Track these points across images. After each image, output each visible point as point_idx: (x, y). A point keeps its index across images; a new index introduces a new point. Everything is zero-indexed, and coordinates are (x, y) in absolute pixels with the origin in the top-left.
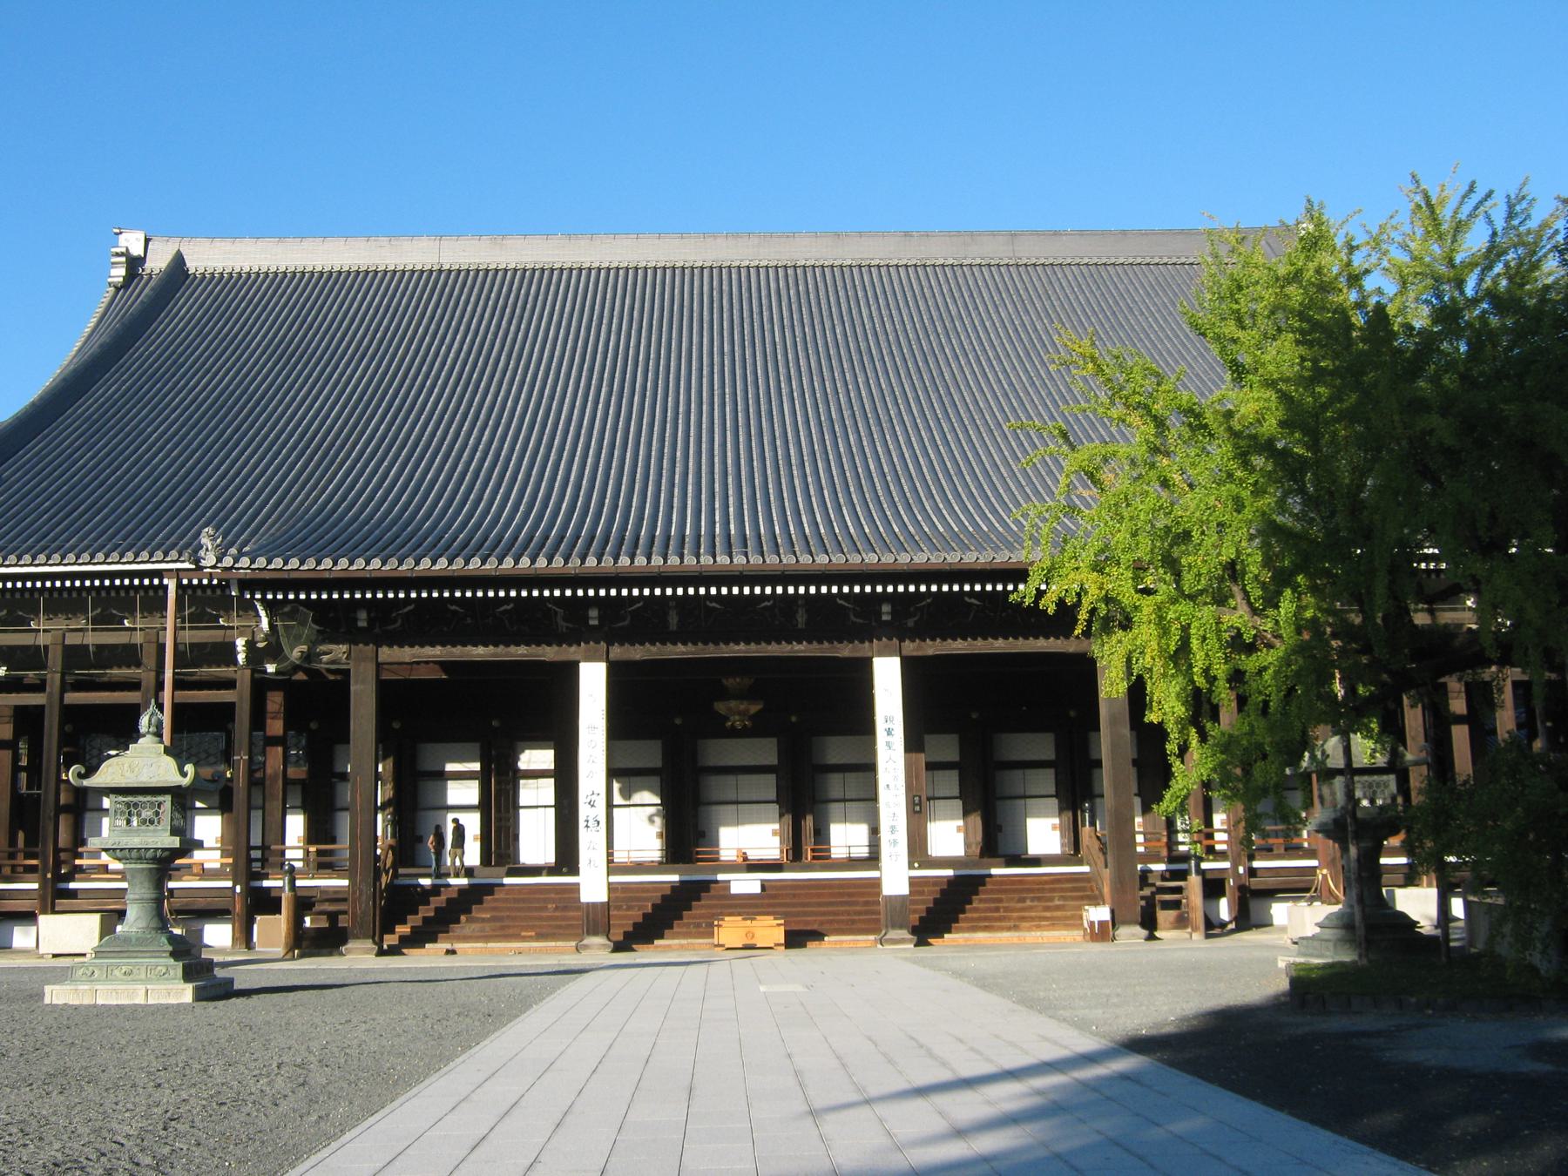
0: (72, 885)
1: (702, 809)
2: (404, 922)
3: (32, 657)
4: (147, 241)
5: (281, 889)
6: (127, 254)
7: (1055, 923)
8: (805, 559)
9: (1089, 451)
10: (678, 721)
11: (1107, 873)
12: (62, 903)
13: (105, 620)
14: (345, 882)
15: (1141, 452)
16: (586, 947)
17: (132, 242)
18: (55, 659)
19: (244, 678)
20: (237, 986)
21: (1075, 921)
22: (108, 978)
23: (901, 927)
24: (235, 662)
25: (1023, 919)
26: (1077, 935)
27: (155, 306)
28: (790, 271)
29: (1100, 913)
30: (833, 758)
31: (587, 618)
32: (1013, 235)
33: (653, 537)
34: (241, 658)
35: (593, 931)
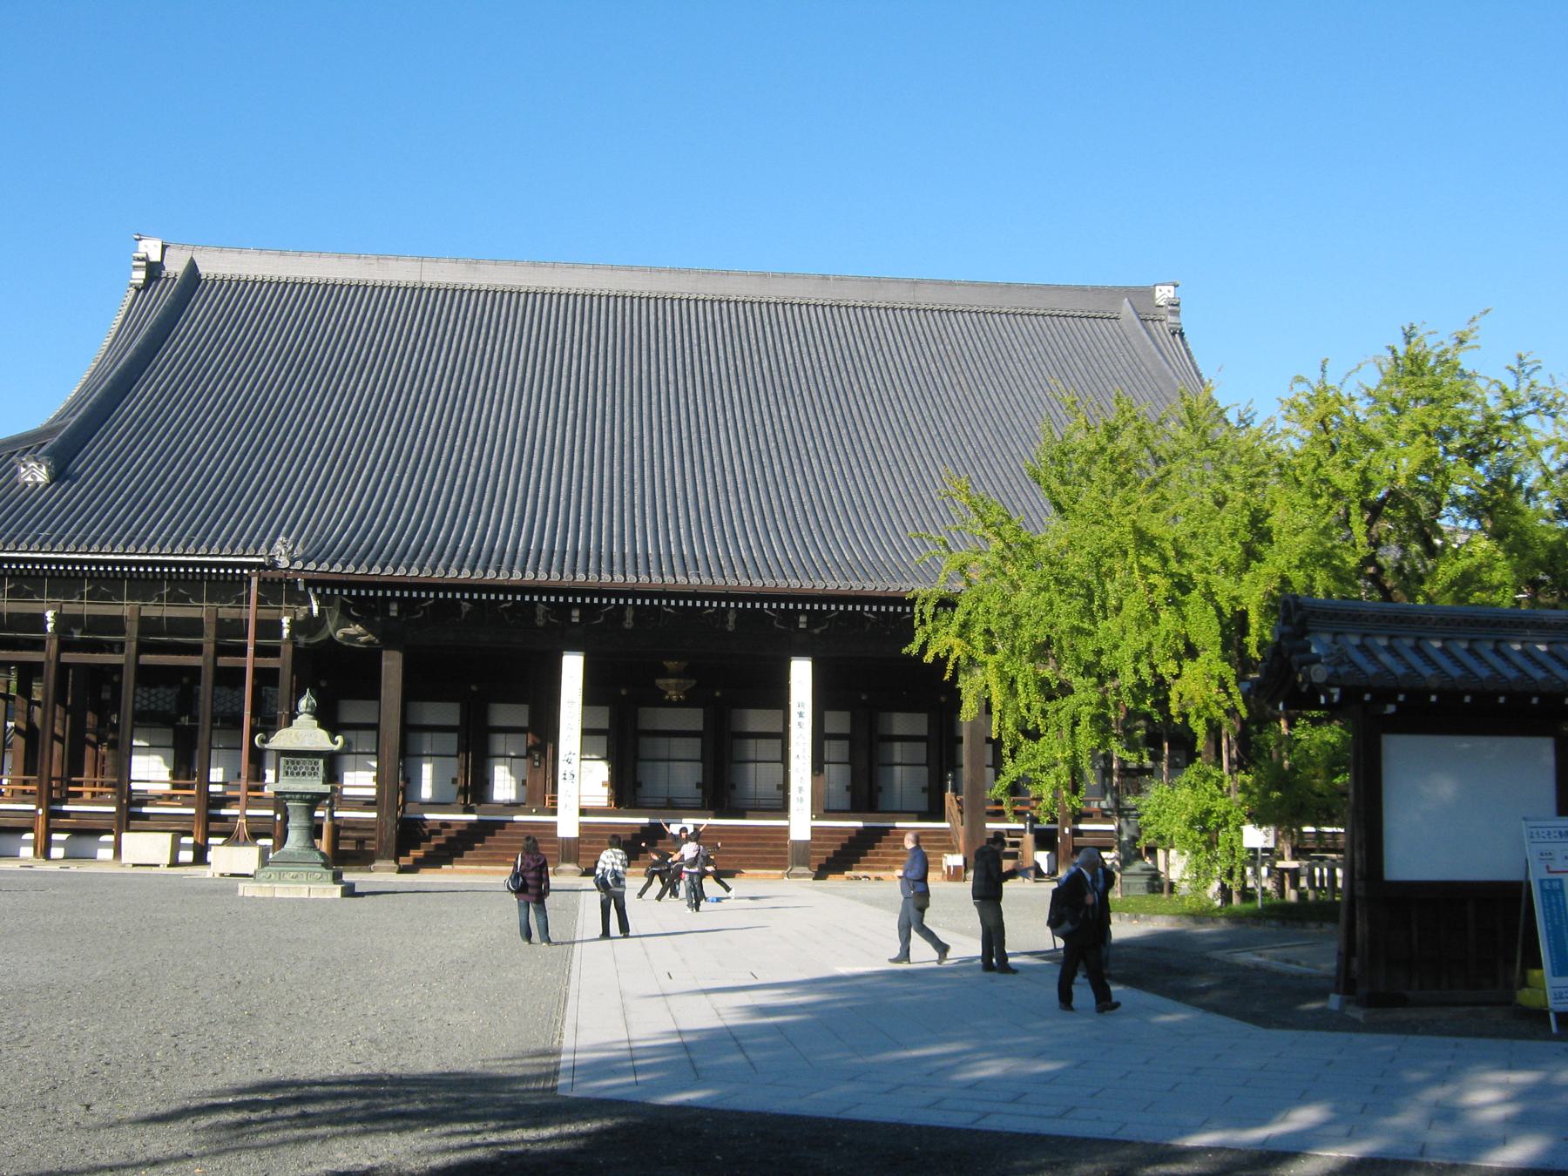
0: (65, 808)
1: (641, 764)
2: (418, 847)
3: (116, 624)
4: (164, 248)
5: (322, 818)
6: (146, 259)
8: (744, 582)
9: (959, 556)
10: (624, 692)
11: (962, 829)
12: (134, 823)
13: (176, 599)
14: (374, 815)
16: (561, 872)
17: (151, 249)
18: (132, 628)
19: (287, 651)
20: (357, 890)
22: (280, 880)
23: (803, 865)
24: (280, 635)
27: (175, 306)
28: (724, 305)
29: (956, 860)
31: (570, 616)
32: (915, 283)
33: (623, 555)
34: (286, 632)
35: (567, 860)
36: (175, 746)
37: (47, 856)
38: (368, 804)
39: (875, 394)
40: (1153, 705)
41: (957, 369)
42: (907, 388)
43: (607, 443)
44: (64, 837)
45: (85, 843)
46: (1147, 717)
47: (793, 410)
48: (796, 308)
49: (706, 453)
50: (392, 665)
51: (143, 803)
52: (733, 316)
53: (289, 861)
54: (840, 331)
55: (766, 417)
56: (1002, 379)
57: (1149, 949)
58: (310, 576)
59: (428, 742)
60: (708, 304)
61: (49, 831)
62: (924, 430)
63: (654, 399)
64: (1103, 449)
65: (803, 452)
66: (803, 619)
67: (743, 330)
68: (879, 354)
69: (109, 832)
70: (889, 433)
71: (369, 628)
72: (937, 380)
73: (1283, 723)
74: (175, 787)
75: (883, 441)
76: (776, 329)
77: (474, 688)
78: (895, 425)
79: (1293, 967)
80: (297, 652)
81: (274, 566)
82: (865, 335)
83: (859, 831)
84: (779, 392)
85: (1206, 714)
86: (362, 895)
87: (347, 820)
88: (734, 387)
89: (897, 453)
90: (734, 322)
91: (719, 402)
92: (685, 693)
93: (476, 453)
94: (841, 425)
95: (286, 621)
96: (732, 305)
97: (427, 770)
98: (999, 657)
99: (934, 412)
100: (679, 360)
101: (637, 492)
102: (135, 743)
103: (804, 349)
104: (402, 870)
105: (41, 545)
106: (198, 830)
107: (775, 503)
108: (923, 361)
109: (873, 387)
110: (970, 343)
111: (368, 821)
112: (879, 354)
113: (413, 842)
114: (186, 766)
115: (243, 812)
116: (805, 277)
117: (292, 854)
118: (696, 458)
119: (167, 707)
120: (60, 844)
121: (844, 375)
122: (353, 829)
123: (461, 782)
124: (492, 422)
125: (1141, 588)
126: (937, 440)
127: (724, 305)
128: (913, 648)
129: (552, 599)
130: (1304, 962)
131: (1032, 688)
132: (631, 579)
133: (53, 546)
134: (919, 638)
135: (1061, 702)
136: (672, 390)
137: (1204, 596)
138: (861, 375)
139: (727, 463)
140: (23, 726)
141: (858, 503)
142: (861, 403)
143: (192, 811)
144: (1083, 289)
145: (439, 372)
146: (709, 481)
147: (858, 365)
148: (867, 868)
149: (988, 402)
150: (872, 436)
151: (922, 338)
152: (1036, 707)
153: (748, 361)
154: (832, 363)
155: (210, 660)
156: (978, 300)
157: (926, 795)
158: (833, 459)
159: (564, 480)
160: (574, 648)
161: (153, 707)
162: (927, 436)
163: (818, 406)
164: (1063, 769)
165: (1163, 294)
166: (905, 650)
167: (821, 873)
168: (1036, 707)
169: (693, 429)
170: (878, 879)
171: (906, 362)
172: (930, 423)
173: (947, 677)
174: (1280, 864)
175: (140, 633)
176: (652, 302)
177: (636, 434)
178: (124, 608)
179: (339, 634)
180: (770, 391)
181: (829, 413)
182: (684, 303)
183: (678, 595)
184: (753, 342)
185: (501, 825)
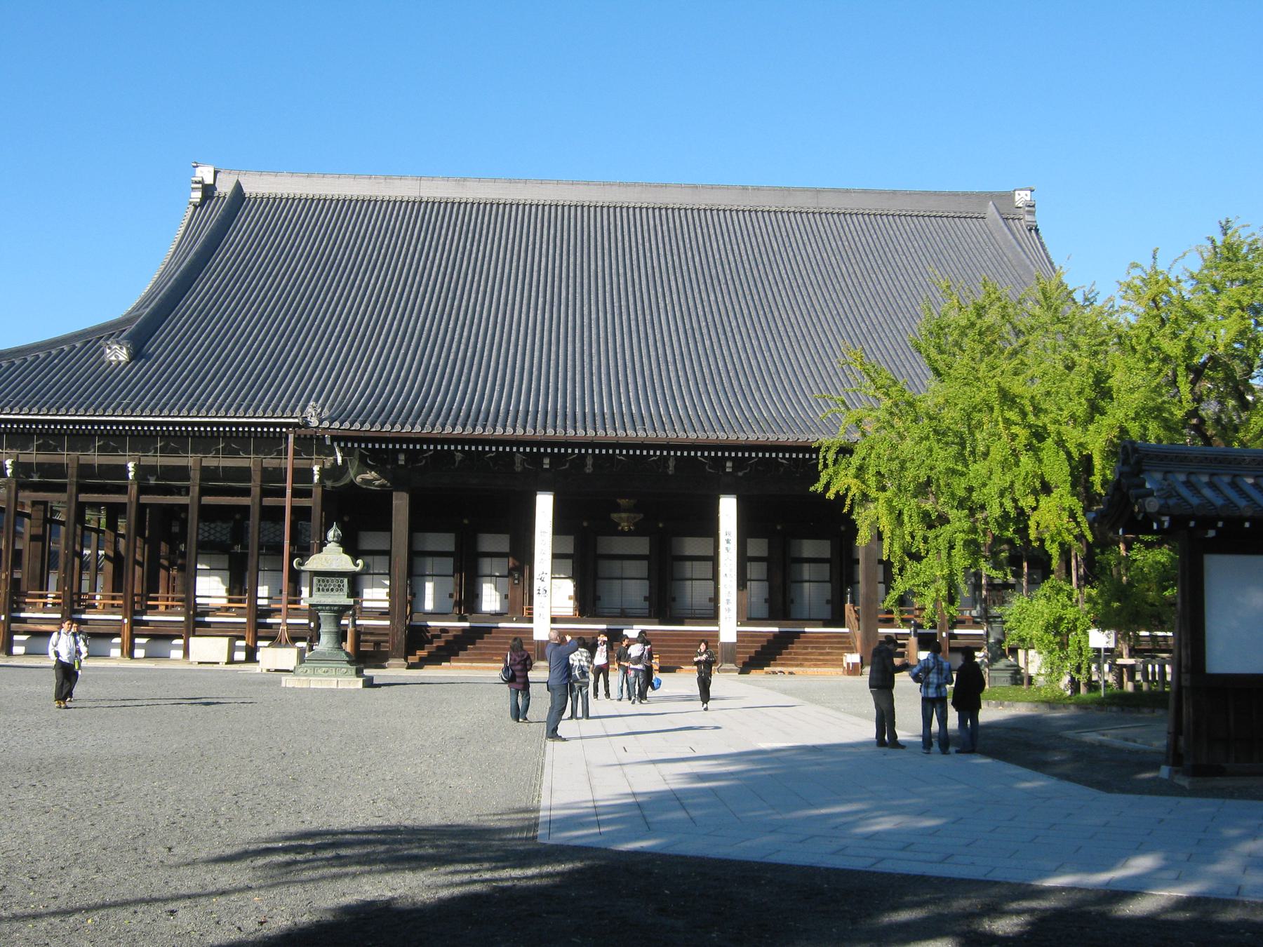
0: (145, 618)
3: (183, 472)
4: (216, 173)
7: (825, 663)
8: (682, 435)
9: (856, 413)
10: (585, 524)
11: (859, 633)
13: (230, 452)
14: (388, 623)
15: (884, 416)
17: (205, 174)
18: (195, 476)
19: (317, 492)
21: (838, 662)
25: (806, 660)
26: (840, 670)
28: (663, 212)
29: (854, 658)
30: (689, 551)
31: (542, 464)
32: (818, 191)
33: (584, 413)
34: (316, 478)
36: (230, 569)
37: (131, 656)
38: (383, 614)
39: (787, 282)
40: (1015, 532)
41: (853, 261)
42: (812, 277)
43: (570, 324)
44: (144, 641)
45: (160, 646)
46: (1010, 541)
47: (719, 296)
48: (721, 213)
49: (650, 331)
50: (401, 503)
51: (206, 614)
52: (671, 220)
53: (322, 659)
54: (758, 231)
55: (698, 301)
56: (889, 269)
57: (1013, 729)
58: (334, 433)
59: (429, 564)
60: (650, 211)
61: (133, 636)
62: (826, 310)
63: (608, 288)
64: (973, 325)
65: (728, 329)
66: (729, 464)
67: (679, 231)
68: (789, 250)
69: (180, 637)
70: (798, 313)
71: (382, 473)
72: (837, 270)
73: (1122, 546)
74: (230, 601)
75: (793, 320)
76: (705, 230)
77: (466, 521)
78: (803, 307)
79: (1131, 745)
80: (326, 495)
81: (306, 425)
82: (778, 234)
83: (775, 635)
84: (709, 281)
85: (1060, 539)
86: (379, 686)
87: (367, 627)
88: (672, 278)
89: (805, 330)
90: (671, 225)
91: (660, 290)
92: (635, 524)
93: (465, 334)
94: (759, 307)
95: (316, 469)
96: (670, 212)
97: (429, 587)
98: (889, 494)
99: (834, 296)
100: (627, 257)
101: (595, 363)
102: (199, 566)
103: (729, 247)
104: (410, 667)
105: (123, 411)
106: (249, 635)
107: (706, 370)
108: (825, 255)
109: (785, 276)
110: (863, 239)
111: (383, 628)
112: (789, 250)
113: (419, 644)
114: (239, 584)
115: (284, 621)
116: (728, 188)
117: (323, 654)
118: (642, 335)
119: (224, 538)
120: (141, 646)
121: (761, 267)
122: (372, 634)
123: (456, 597)
124: (478, 308)
125: (1005, 438)
126: (837, 319)
127: (663, 212)
128: (819, 487)
129: (528, 449)
130: (1140, 741)
131: (915, 519)
132: (591, 433)
133: (133, 411)
134: (824, 479)
135: (939, 530)
136: (622, 281)
137: (1056, 443)
138: (774, 266)
139: (666, 339)
140: (111, 554)
141: (773, 370)
142: (775, 289)
143: (244, 620)
144: (956, 194)
145: (435, 269)
146: (653, 353)
147: (772, 259)
148: (783, 665)
149: (878, 287)
150: (784, 316)
151: (824, 236)
152: (919, 534)
153: (683, 256)
154: (751, 257)
155: (257, 500)
156: (870, 204)
157: (829, 607)
158: (753, 335)
159: (536, 354)
160: (545, 489)
161: (212, 538)
162: (828, 316)
163: (740, 292)
164: (942, 585)
165: (1022, 197)
166: (812, 489)
167: (746, 668)
168: (919, 534)
169: (639, 312)
170: (791, 673)
171: (811, 256)
172: (831, 305)
173: (845, 510)
174: (1119, 661)
175: (201, 479)
176: (605, 210)
177: (593, 316)
178: (189, 460)
179: (359, 479)
180: (701, 281)
181: (749, 298)
182: (631, 211)
183: (628, 446)
184: (687, 241)
185: (489, 630)
